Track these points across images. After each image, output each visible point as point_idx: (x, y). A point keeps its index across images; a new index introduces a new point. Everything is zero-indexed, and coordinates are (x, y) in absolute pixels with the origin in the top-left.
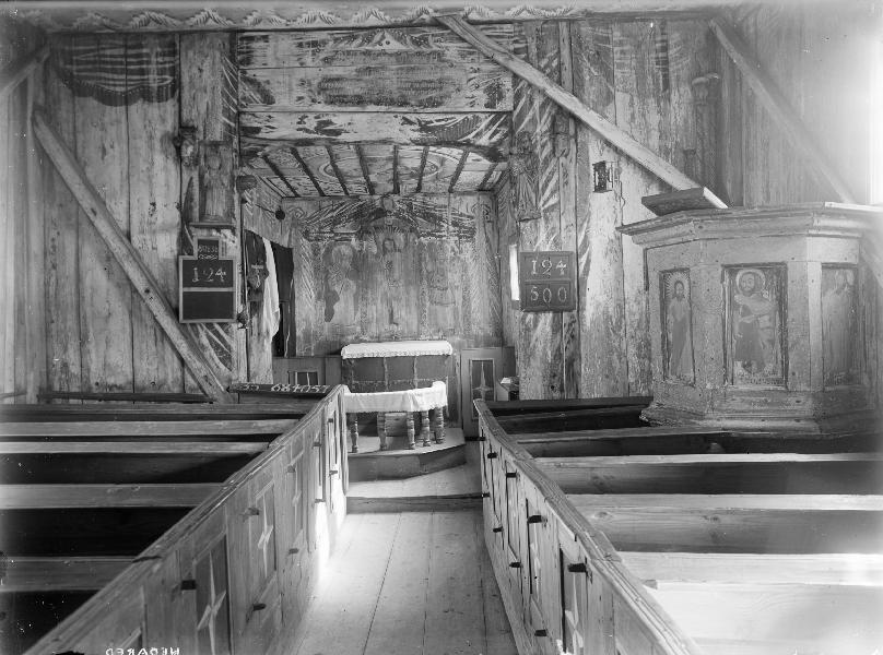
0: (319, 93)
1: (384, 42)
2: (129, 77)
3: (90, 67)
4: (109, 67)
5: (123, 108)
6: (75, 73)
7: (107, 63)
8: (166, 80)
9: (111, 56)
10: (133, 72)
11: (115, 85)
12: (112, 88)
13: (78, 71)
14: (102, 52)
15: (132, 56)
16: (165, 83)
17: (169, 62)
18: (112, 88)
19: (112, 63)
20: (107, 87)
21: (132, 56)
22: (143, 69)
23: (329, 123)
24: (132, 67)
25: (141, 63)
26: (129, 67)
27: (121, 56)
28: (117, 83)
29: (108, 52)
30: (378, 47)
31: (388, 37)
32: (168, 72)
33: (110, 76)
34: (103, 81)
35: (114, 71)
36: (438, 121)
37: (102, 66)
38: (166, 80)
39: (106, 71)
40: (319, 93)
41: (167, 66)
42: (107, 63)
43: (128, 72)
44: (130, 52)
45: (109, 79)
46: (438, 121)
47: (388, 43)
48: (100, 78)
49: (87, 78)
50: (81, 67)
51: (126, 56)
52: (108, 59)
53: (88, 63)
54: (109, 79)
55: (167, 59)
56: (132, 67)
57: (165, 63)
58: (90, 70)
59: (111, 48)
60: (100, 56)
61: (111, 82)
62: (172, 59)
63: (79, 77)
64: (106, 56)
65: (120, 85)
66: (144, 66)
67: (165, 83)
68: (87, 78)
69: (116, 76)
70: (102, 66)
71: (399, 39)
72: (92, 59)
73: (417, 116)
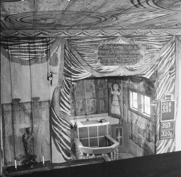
0: (98, 59)
1: (119, 41)
2: (30, 54)
3: (15, 51)
4: (23, 50)
5: (29, 66)
6: (10, 53)
7: (22, 49)
8: (44, 55)
9: (24, 46)
10: (32, 53)
11: (25, 58)
12: (24, 59)
13: (11, 52)
14: (20, 45)
15: (31, 46)
16: (44, 56)
17: (45, 49)
18: (24, 59)
19: (25, 49)
20: (23, 59)
21: (31, 46)
22: (35, 51)
23: (101, 69)
24: (32, 51)
25: (35, 49)
26: (30, 51)
27: (27, 46)
28: (26, 57)
29: (23, 45)
30: (118, 43)
31: (121, 40)
32: (44, 52)
33: (24, 54)
34: (21, 56)
35: (25, 52)
36: (135, 68)
37: (21, 50)
38: (44, 55)
39: (22, 52)
40: (98, 59)
41: (44, 50)
42: (22, 49)
43: (30, 52)
44: (31, 45)
45: (23, 55)
46: (135, 68)
47: (121, 41)
48: (20, 55)
49: (15, 55)
50: (12, 51)
51: (29, 46)
52: (23, 48)
53: (14, 49)
54: (23, 55)
55: (44, 47)
56: (32, 51)
57: (44, 49)
58: (17, 52)
59: (23, 43)
60: (20, 46)
61: (24, 57)
62: (46, 47)
63: (12, 55)
64: (21, 46)
65: (27, 58)
66: (36, 50)
67: (44, 56)
68: (15, 55)
69: (25, 54)
70: (21, 50)
71: (124, 40)
72: (17, 48)
73: (129, 66)
